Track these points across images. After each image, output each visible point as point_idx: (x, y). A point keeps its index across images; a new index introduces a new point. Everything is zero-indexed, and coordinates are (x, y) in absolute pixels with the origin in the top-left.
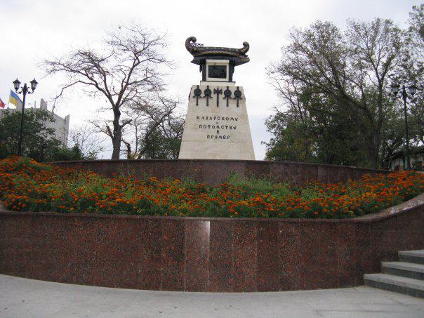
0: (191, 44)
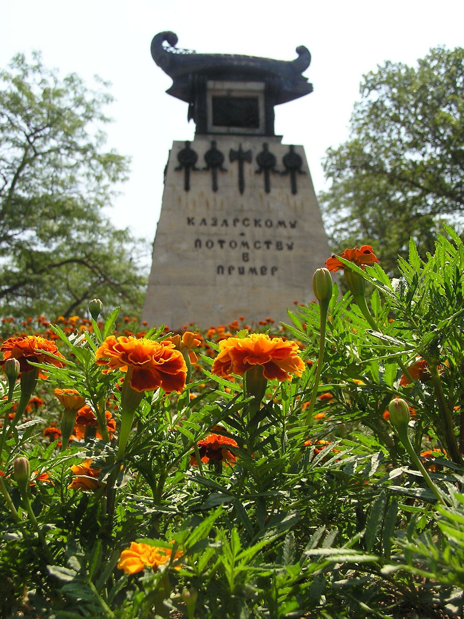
0: (163, 50)
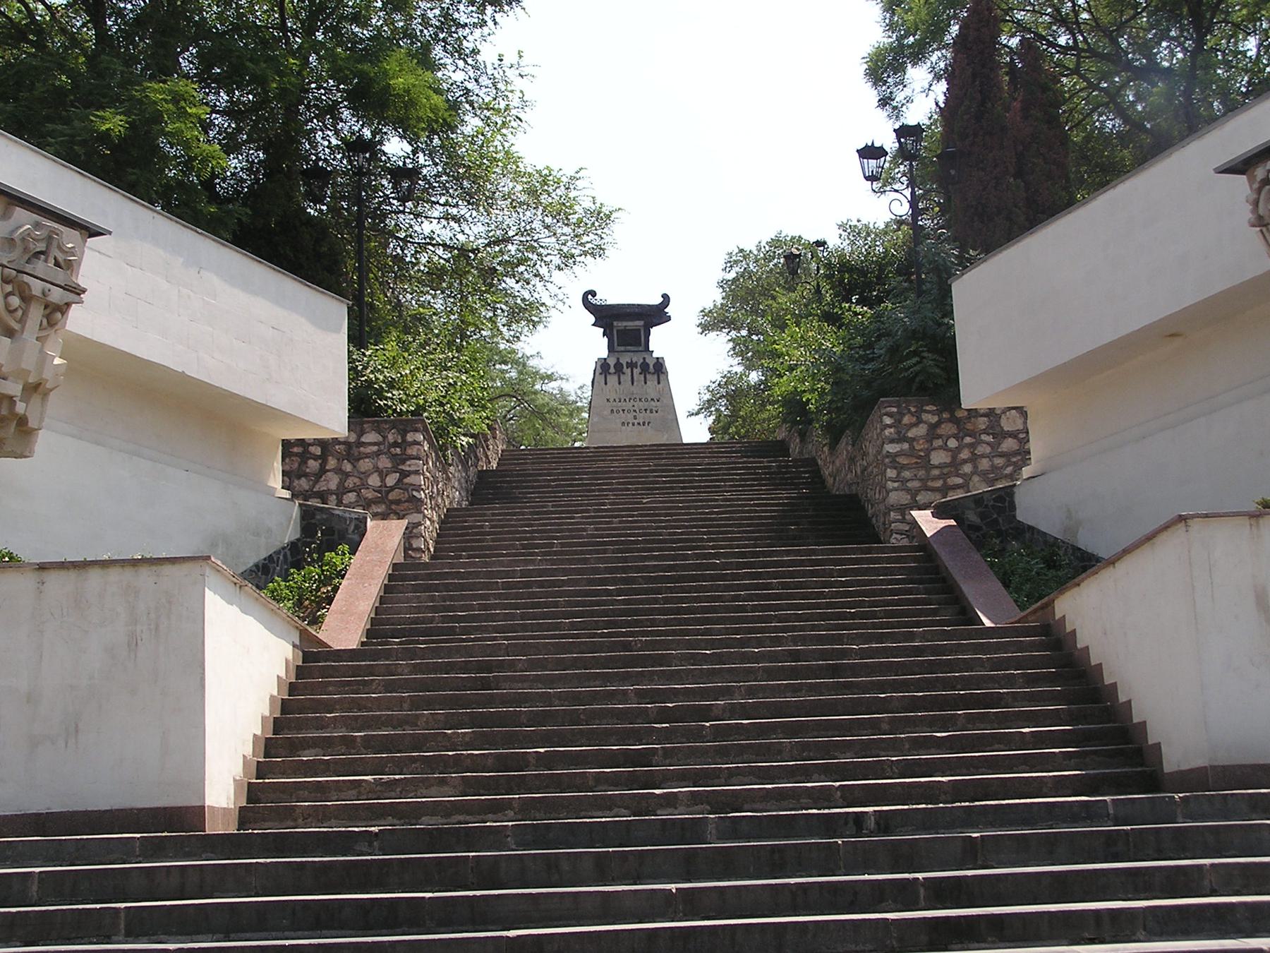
0: (588, 299)
